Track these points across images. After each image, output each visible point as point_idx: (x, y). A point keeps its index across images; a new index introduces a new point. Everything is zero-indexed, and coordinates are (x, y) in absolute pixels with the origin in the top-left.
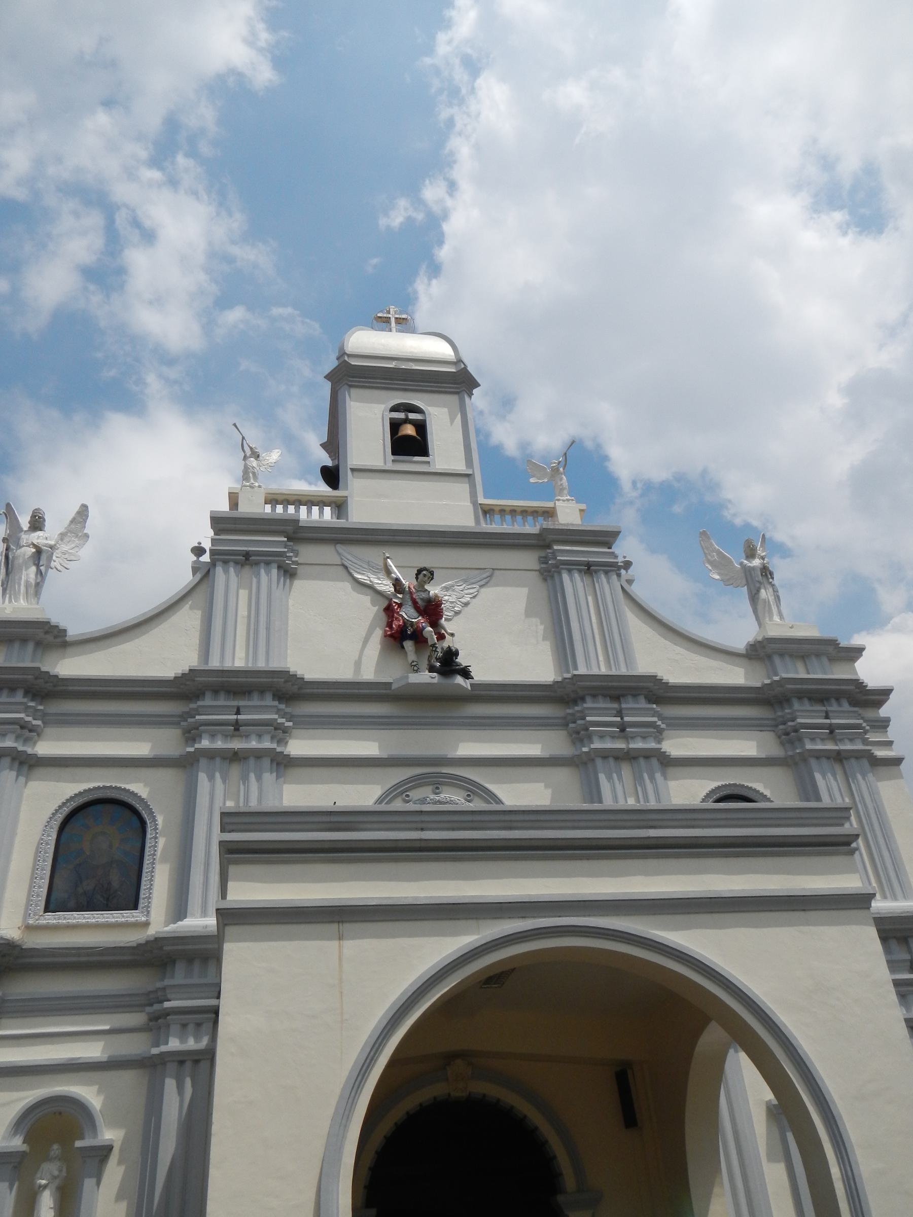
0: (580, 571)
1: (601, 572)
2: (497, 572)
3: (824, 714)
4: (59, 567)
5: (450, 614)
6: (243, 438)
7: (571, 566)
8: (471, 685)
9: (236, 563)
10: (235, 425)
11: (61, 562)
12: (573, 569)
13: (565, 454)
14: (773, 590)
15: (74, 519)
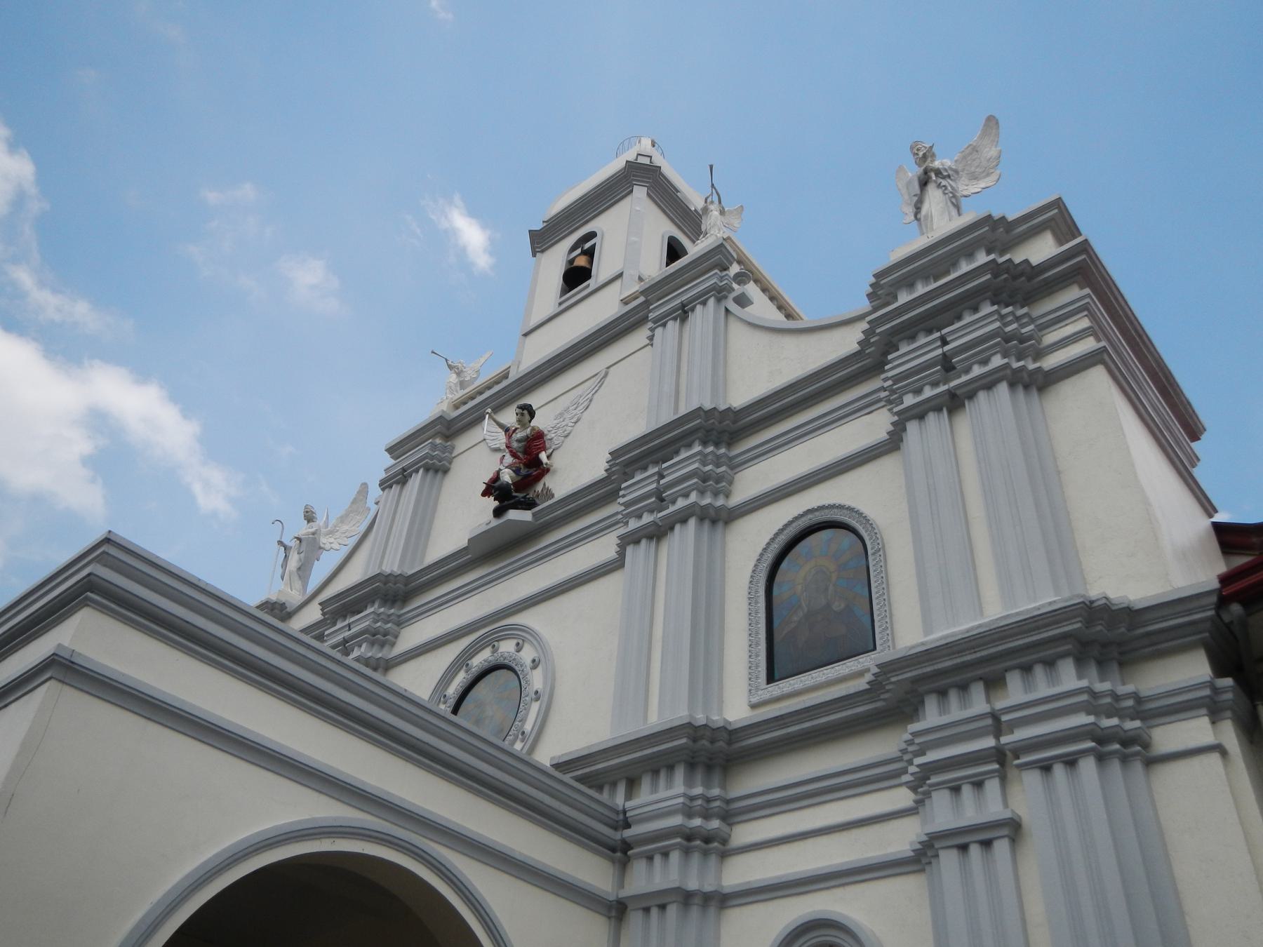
0: (675, 319)
1: (698, 306)
2: (612, 369)
3: (939, 343)
4: (336, 546)
5: (558, 442)
6: (446, 360)
7: (661, 322)
8: (534, 515)
9: (397, 482)
10: (433, 352)
11: (340, 541)
12: (666, 322)
13: (713, 185)
14: (945, 194)
15: (355, 499)
